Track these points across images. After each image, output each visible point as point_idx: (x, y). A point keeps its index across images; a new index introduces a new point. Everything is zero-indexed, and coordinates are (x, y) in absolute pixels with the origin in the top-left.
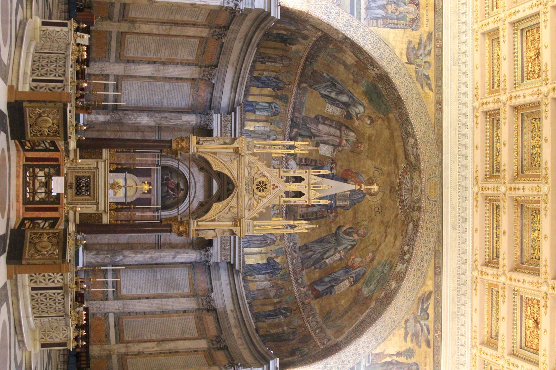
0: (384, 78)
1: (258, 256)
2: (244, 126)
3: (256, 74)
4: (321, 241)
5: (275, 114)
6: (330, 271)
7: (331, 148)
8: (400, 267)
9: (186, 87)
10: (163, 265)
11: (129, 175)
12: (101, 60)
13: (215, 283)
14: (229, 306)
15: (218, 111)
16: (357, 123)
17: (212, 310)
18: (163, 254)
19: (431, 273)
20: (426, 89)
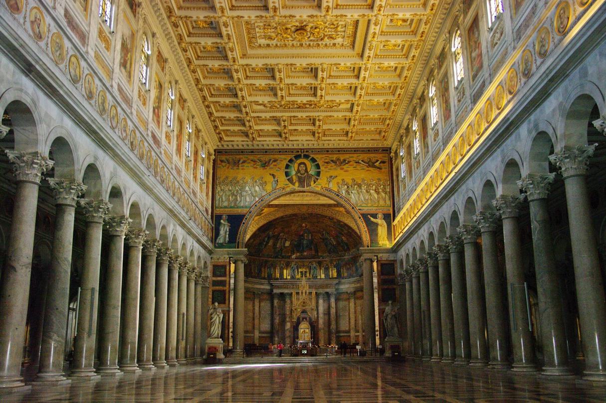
0: (259, 229)
1: (333, 271)
2: (278, 279)
3: (256, 275)
4: (326, 246)
5: (272, 265)
6: (338, 243)
7: (287, 242)
8: (335, 220)
9: (262, 304)
10: (336, 312)
11: (299, 327)
12: (254, 339)
13: (344, 290)
14: (353, 285)
15: (272, 290)
16: (276, 233)
17: (355, 293)
18: (331, 313)
19: (337, 209)
20: (264, 211)
